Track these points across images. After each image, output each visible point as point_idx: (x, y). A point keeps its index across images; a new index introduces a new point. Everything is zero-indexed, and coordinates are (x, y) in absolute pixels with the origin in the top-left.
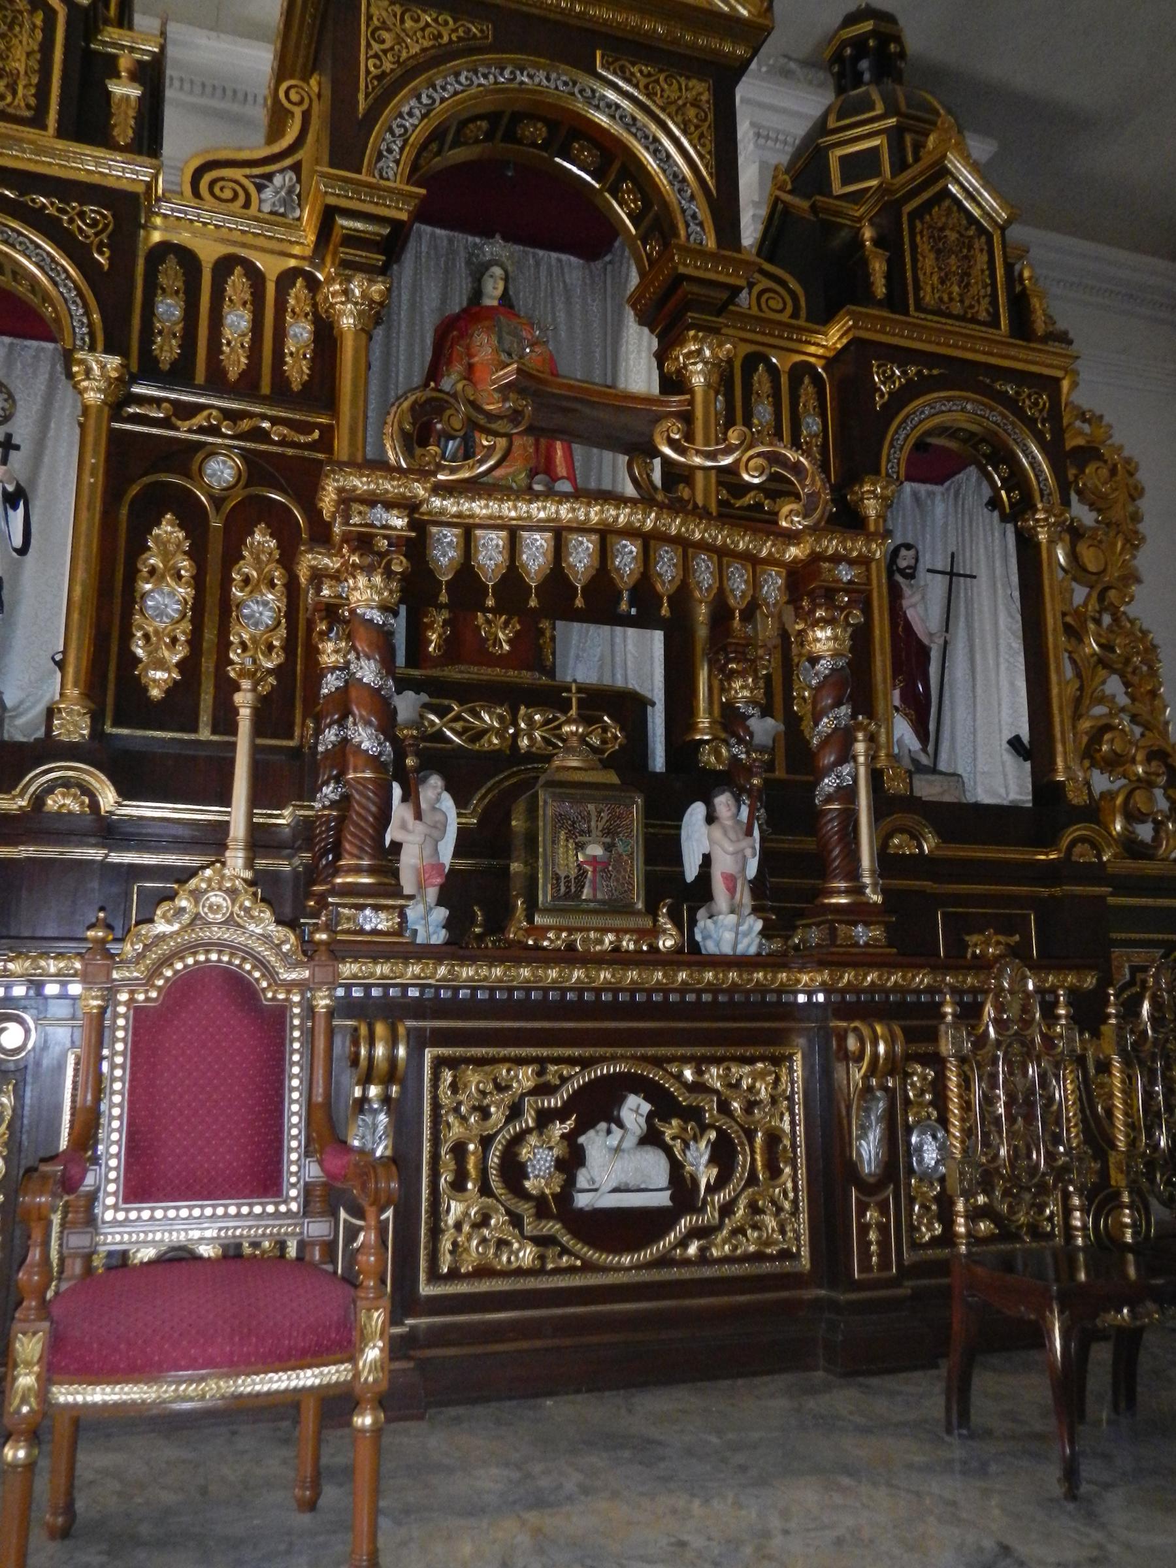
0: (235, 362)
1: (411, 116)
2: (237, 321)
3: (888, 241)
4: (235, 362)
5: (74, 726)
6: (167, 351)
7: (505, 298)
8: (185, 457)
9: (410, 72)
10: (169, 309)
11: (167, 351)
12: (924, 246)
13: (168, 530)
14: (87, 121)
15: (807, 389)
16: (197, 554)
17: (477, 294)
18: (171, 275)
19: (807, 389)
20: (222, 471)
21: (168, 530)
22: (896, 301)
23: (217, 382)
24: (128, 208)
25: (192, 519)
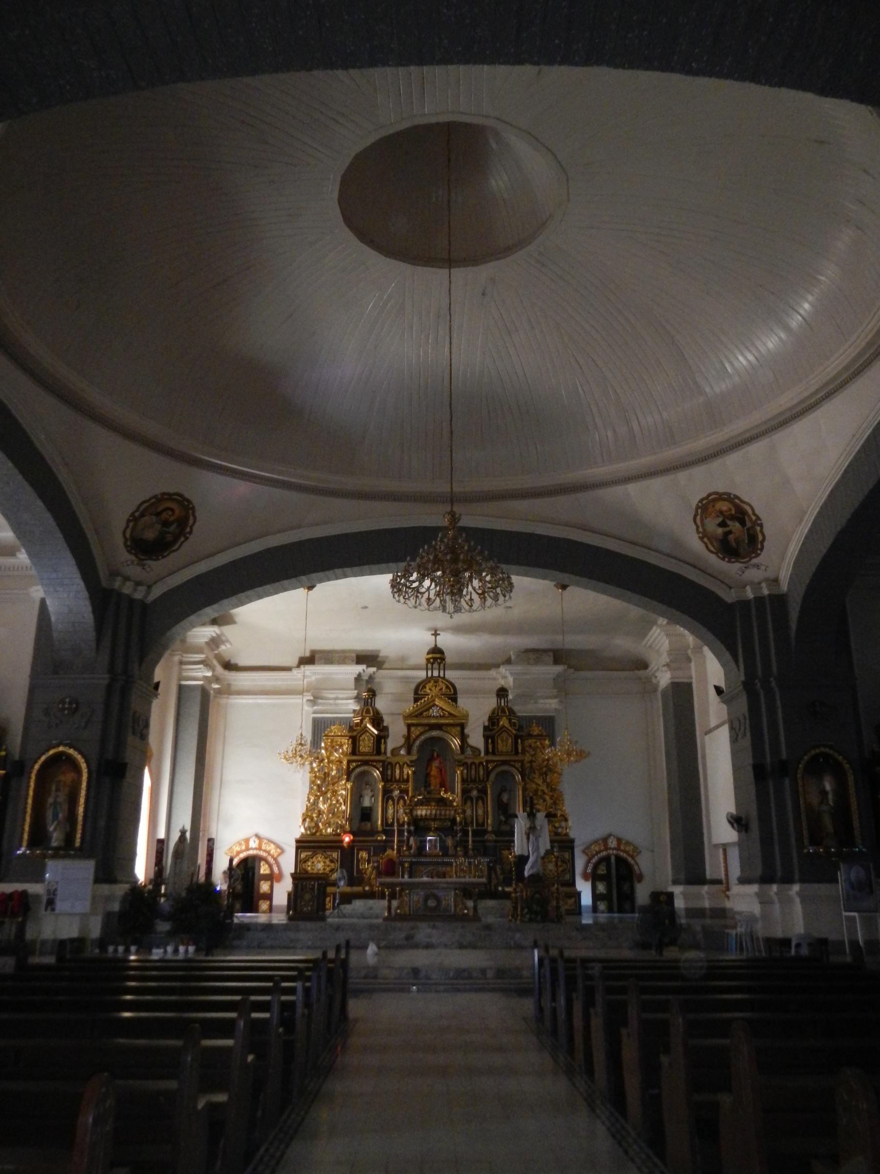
0: (398, 777)
1: (418, 743)
2: (398, 772)
3: (493, 742)
4: (398, 777)
5: (380, 828)
6: (389, 778)
7: (438, 756)
8: (392, 791)
9: (418, 737)
10: (389, 772)
11: (389, 778)
12: (500, 742)
13: (390, 802)
14: (379, 752)
15: (481, 768)
16: (394, 804)
17: (433, 755)
18: (389, 767)
19: (481, 768)
20: (396, 793)
21: (390, 802)
22: (493, 753)
23: (396, 781)
24: (383, 762)
25: (393, 801)
